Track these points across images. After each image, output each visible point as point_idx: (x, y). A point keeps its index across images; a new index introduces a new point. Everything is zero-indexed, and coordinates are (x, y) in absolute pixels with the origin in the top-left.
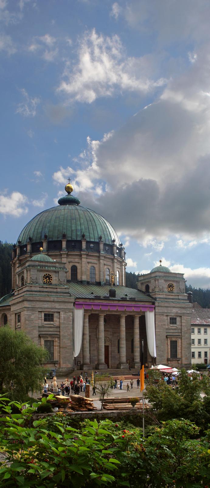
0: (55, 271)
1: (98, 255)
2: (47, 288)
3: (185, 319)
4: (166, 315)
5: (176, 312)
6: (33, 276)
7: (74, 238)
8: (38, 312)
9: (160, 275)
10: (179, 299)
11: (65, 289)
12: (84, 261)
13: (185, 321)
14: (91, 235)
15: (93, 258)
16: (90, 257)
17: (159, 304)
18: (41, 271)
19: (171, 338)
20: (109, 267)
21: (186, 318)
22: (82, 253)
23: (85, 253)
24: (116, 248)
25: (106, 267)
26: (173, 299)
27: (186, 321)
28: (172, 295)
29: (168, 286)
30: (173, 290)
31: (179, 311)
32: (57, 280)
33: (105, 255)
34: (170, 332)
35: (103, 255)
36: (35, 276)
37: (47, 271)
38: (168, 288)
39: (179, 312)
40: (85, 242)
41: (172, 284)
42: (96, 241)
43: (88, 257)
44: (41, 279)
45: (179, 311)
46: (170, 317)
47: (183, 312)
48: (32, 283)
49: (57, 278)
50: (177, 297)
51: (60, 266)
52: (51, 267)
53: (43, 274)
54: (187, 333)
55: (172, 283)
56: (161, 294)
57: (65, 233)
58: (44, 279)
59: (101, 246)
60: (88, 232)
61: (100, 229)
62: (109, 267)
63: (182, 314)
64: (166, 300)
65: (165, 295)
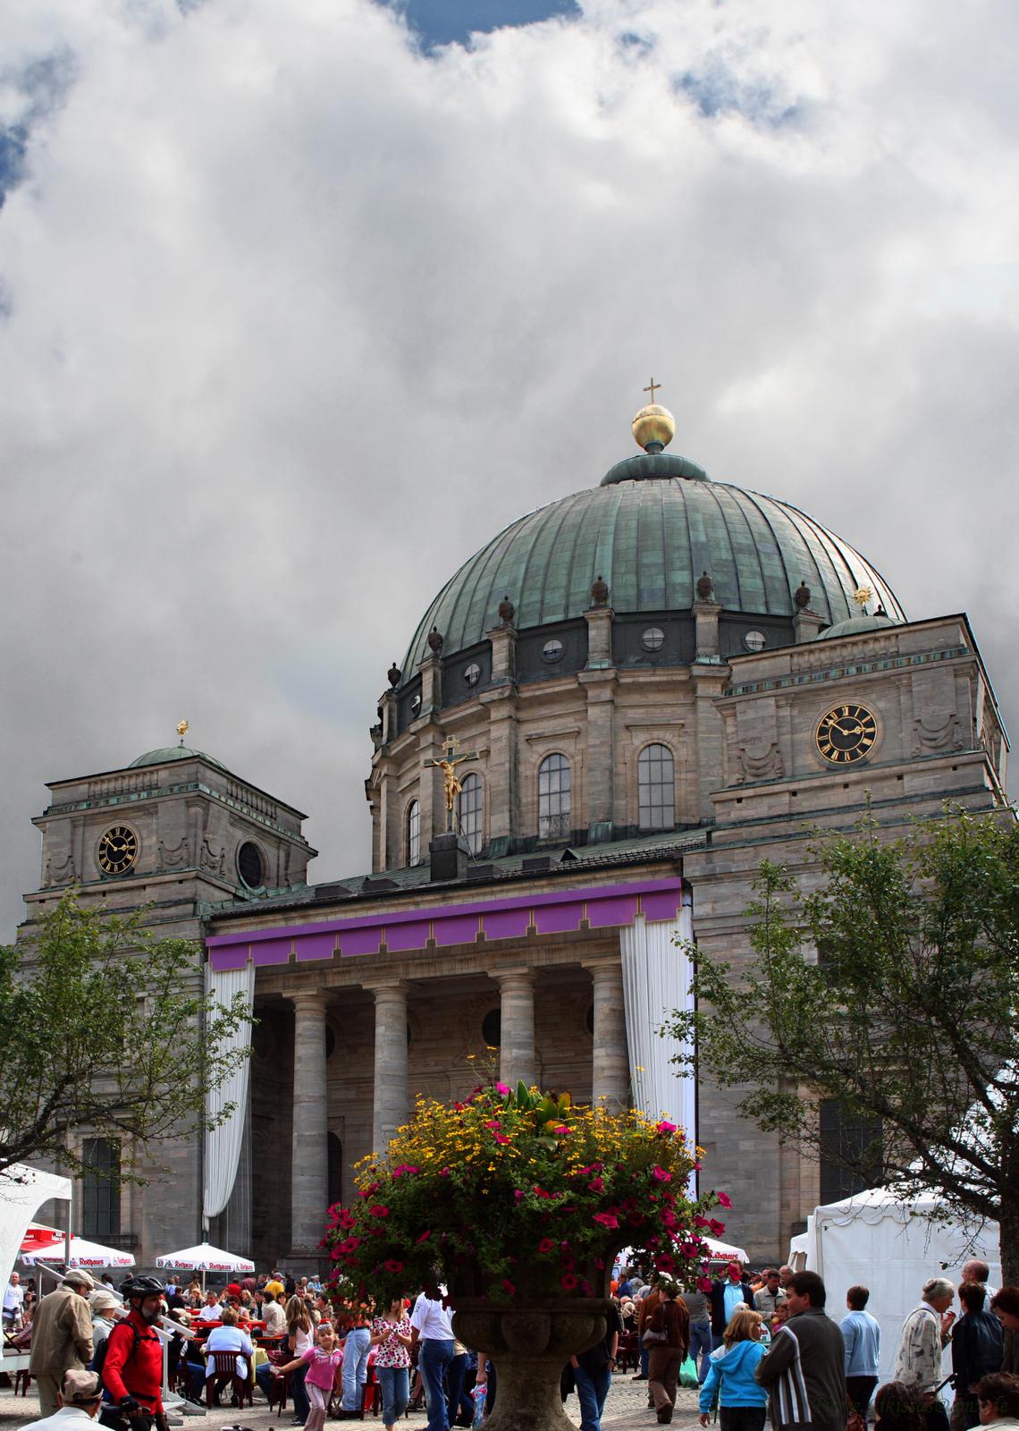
0: (143, 806)
1: (575, 686)
2: (104, 893)
6: (55, 851)
7: (472, 638)
9: (757, 676)
10: (904, 800)
11: (181, 882)
12: (498, 739)
14: (548, 598)
15: (557, 709)
16: (544, 711)
17: (710, 861)
18: (90, 821)
20: (667, 736)
22: (485, 697)
23: (495, 695)
24: (714, 619)
25: (640, 739)
26: (847, 809)
28: (846, 786)
29: (823, 731)
30: (864, 748)
32: (155, 849)
33: (611, 675)
35: (597, 676)
36: (66, 850)
37: (115, 814)
38: (822, 744)
40: (506, 642)
41: (852, 710)
42: (572, 615)
43: (523, 715)
44: (91, 861)
48: (53, 883)
49: (154, 839)
50: (889, 790)
51: (175, 780)
52: (130, 792)
53: (98, 834)
55: (854, 703)
56: (750, 792)
57: (443, 634)
58: (102, 857)
59: (592, 633)
60: (539, 585)
61: (616, 553)
62: (667, 736)
64: (782, 828)
65: (786, 798)
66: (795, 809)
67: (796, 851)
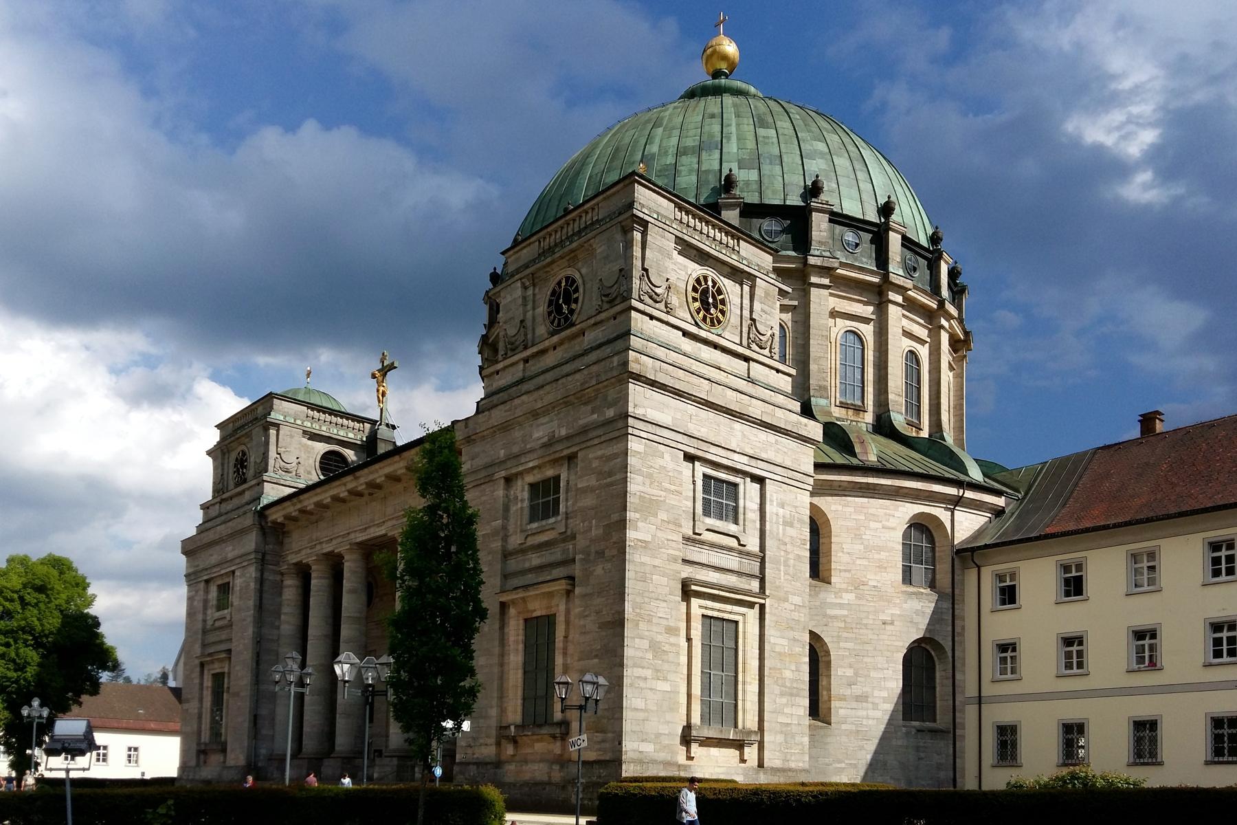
3: (595, 464)
4: (503, 474)
5: (546, 439)
8: (202, 584)
13: (592, 481)
19: (523, 599)
21: (600, 458)
27: (601, 474)
31: (559, 426)
34: (527, 565)
39: (563, 432)
45: (559, 426)
46: (530, 479)
47: (581, 422)
54: (600, 554)
63: (577, 440)
66: (528, 374)
67: (510, 410)
